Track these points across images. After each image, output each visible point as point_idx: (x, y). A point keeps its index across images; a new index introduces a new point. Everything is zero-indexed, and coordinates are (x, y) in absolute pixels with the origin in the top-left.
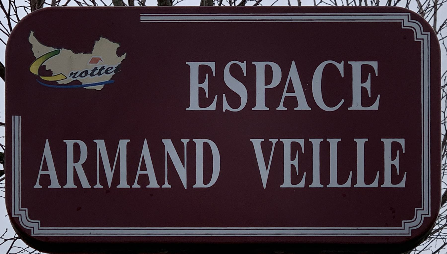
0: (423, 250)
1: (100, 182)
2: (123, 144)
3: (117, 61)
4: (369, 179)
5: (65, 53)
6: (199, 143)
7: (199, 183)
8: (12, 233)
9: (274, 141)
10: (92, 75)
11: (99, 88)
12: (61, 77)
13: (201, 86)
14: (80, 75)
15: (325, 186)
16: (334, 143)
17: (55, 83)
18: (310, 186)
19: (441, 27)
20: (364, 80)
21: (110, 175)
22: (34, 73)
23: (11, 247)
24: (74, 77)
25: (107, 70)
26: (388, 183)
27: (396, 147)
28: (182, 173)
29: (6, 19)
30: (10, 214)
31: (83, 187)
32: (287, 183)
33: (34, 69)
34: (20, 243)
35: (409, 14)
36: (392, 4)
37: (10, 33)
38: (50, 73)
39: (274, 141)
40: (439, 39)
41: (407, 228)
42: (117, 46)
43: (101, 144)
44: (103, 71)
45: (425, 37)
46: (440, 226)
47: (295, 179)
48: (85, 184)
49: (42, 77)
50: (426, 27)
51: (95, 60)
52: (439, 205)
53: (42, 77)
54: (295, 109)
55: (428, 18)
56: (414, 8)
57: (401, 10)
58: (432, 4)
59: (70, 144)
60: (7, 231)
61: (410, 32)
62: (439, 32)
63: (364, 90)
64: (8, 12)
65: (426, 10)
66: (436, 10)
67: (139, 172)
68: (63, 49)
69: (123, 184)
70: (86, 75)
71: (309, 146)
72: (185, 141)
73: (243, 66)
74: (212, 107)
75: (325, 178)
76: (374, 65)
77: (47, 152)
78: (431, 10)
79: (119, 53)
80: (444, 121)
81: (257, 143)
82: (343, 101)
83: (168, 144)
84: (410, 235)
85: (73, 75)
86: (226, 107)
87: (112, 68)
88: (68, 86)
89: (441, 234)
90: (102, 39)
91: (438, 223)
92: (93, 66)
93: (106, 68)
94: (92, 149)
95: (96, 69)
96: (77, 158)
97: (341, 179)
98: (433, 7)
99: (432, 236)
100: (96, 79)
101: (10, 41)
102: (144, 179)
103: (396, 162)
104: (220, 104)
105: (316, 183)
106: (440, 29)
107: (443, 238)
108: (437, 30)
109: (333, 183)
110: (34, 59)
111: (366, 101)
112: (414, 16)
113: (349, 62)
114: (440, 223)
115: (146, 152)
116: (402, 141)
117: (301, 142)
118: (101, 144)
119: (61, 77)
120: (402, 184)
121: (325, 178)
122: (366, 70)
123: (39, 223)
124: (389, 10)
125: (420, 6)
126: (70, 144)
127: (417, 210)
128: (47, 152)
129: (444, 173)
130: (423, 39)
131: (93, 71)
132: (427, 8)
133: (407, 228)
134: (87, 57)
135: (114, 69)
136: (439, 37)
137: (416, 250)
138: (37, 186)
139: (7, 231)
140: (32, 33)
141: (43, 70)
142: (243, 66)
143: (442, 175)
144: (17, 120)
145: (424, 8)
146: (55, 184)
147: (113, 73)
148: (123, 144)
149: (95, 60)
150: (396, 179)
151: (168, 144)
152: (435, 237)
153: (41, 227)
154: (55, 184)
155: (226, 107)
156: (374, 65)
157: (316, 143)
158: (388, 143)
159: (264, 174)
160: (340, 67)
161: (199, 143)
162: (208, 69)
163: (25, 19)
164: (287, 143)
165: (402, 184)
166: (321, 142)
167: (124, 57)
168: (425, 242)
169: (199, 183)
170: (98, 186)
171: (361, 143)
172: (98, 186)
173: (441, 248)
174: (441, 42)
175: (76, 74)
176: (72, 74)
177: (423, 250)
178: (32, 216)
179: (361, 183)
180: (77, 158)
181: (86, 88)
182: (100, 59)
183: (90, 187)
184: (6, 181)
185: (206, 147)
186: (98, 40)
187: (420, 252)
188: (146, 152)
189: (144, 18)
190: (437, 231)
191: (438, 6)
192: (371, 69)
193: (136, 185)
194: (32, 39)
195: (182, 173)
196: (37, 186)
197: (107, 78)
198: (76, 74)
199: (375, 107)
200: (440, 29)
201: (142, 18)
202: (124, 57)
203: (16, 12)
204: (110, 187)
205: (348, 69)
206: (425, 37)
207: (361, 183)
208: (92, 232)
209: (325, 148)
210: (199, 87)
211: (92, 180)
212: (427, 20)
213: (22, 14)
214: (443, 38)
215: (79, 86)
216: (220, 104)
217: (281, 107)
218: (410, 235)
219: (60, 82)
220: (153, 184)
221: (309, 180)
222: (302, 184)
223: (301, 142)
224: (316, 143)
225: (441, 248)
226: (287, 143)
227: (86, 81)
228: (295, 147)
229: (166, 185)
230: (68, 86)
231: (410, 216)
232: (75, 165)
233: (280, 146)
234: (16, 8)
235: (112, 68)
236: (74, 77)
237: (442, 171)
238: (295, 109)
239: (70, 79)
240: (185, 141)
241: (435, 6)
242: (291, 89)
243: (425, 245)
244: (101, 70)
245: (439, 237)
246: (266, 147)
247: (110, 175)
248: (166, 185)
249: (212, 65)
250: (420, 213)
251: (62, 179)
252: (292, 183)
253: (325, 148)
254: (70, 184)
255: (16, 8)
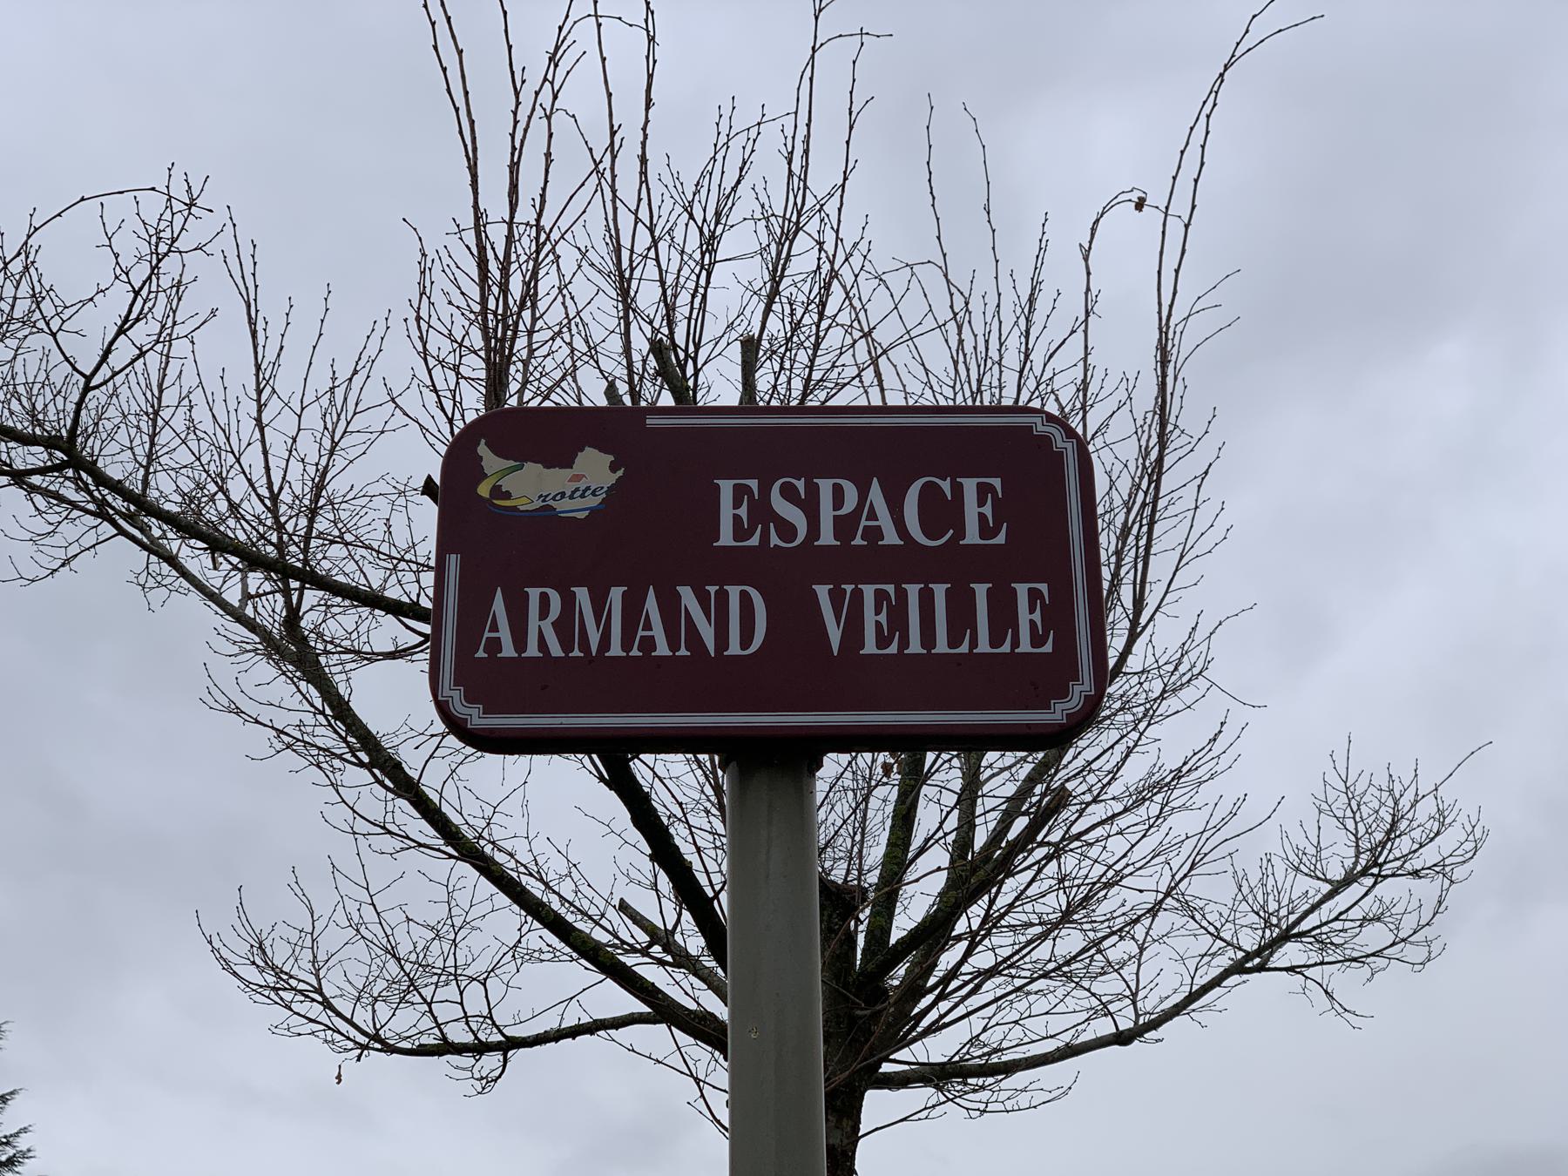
0: (1088, 746)
1: (579, 647)
2: (616, 594)
3: (612, 478)
4: (996, 641)
5: (532, 469)
6: (734, 592)
7: (734, 648)
8: (440, 727)
9: (849, 588)
10: (571, 497)
11: (582, 515)
12: (525, 500)
13: (737, 512)
14: (554, 499)
15: (929, 651)
16: (940, 590)
17: (515, 508)
18: (906, 652)
19: (1094, 435)
20: (981, 503)
21: (594, 638)
22: (484, 495)
23: (438, 747)
24: (544, 501)
25: (595, 491)
26: (1025, 646)
27: (1034, 595)
28: (708, 633)
29: (448, 425)
30: (435, 695)
31: (553, 655)
32: (870, 647)
33: (484, 490)
34: (452, 741)
35: (1044, 415)
36: (1021, 404)
37: (451, 440)
38: (507, 496)
39: (849, 588)
40: (1091, 451)
41: (1058, 711)
42: (611, 458)
43: (582, 594)
44: (589, 492)
45: (1069, 446)
46: (1113, 711)
47: (883, 641)
48: (556, 650)
49: (495, 502)
50: (1070, 433)
51: (577, 478)
52: (1105, 681)
53: (495, 502)
54: (880, 543)
55: (1075, 423)
56: (1052, 408)
57: (1027, 410)
58: (1078, 405)
59: (534, 593)
60: (432, 724)
61: (1046, 440)
62: (1092, 442)
63: (982, 517)
64: (450, 416)
65: (1070, 414)
66: (1085, 413)
67: (641, 633)
68: (529, 463)
69: (616, 650)
70: (563, 497)
71: (902, 596)
72: (712, 589)
73: (800, 485)
74: (754, 541)
75: (928, 637)
76: (997, 482)
77: (499, 606)
78: (1078, 413)
79: (613, 468)
80: (1107, 562)
81: (822, 591)
82: (951, 531)
83: (687, 595)
84: (1065, 721)
85: (544, 498)
86: (775, 540)
87: (602, 488)
88: (534, 514)
89: (1114, 722)
90: (588, 449)
91: (1110, 707)
92: (574, 485)
93: (593, 489)
94: (569, 602)
95: (577, 489)
96: (544, 612)
97: (954, 641)
98: (1081, 409)
99: (1101, 726)
100: (578, 503)
101: (449, 453)
102: (649, 644)
103: (1037, 617)
104: (765, 536)
105: (915, 647)
106: (1092, 438)
107: (1118, 729)
108: (1088, 440)
109: (942, 646)
110: (486, 476)
111: (986, 531)
112: (1050, 418)
113: (958, 480)
114: (1112, 706)
115: (651, 604)
116: (1044, 587)
117: (890, 588)
118: (582, 594)
119: (525, 500)
120: (1048, 648)
121: (928, 637)
122: (983, 491)
123: (481, 709)
124: (1015, 409)
125: (1062, 409)
126: (534, 593)
127: (1073, 685)
128: (499, 606)
129: (1112, 634)
130: (1066, 449)
131: (573, 492)
132: (1072, 411)
133: (1058, 711)
134: (567, 473)
135: (605, 489)
136: (1091, 448)
137: (1077, 746)
138: (481, 654)
139: (432, 724)
140: (483, 441)
141: (497, 492)
142: (800, 485)
143: (1109, 638)
144: (453, 560)
145: (1067, 410)
146: (508, 650)
147: (604, 495)
148: (616, 594)
149: (577, 478)
150: (1037, 640)
151: (687, 595)
152: (1106, 726)
153: (483, 714)
154: (508, 650)
155: (775, 540)
156: (997, 482)
157: (913, 590)
158: (1022, 590)
159: (835, 635)
160: (946, 486)
161: (734, 592)
162: (748, 489)
163: (474, 422)
164: (869, 591)
165: (1048, 648)
166: (921, 588)
167: (620, 473)
168: (1090, 734)
169: (734, 648)
170: (576, 653)
171: (981, 590)
172: (576, 653)
173: (1117, 742)
174: (1094, 456)
175: (546, 496)
176: (541, 496)
177: (1088, 746)
178: (470, 698)
179: (984, 646)
180: (544, 612)
181: (562, 515)
182: (584, 476)
183: (564, 655)
184: (431, 651)
185: (745, 597)
186: (582, 450)
187: (1084, 749)
188: (651, 604)
189: (651, 421)
190: (1108, 717)
191: (1088, 408)
192: (992, 488)
193: (635, 652)
194: (483, 449)
195: (708, 633)
196: (481, 654)
197: (593, 502)
198: (546, 496)
199: (1000, 539)
200: (1092, 438)
201: (648, 421)
202: (620, 473)
203: (463, 416)
204: (594, 654)
205: (958, 490)
206: (1069, 446)
207: (984, 646)
208: (564, 721)
209: (927, 600)
210: (734, 514)
211: (566, 645)
212: (1073, 425)
213: (471, 417)
214: (1097, 450)
215: (553, 513)
216: (765, 536)
217: (858, 541)
218: (1065, 721)
219: (521, 508)
220: (662, 649)
221: (904, 643)
222: (893, 649)
223: (890, 588)
224: (913, 590)
225: (1117, 742)
226: (869, 591)
227: (562, 506)
228: (880, 596)
229: (683, 652)
230: (534, 514)
231: (1063, 693)
232: (541, 623)
233: (858, 596)
234: (463, 410)
235: (602, 488)
236: (544, 501)
237: (1109, 633)
238: (880, 543)
239: (539, 504)
240: (712, 589)
241: (1083, 407)
242: (872, 515)
243: (1092, 739)
244: (585, 491)
245: (1112, 726)
246: (836, 598)
247: (594, 638)
248: (683, 652)
249: (753, 484)
250: (1077, 689)
251: (520, 641)
252: (878, 647)
253: (927, 600)
254: (532, 650)
255: (463, 410)
